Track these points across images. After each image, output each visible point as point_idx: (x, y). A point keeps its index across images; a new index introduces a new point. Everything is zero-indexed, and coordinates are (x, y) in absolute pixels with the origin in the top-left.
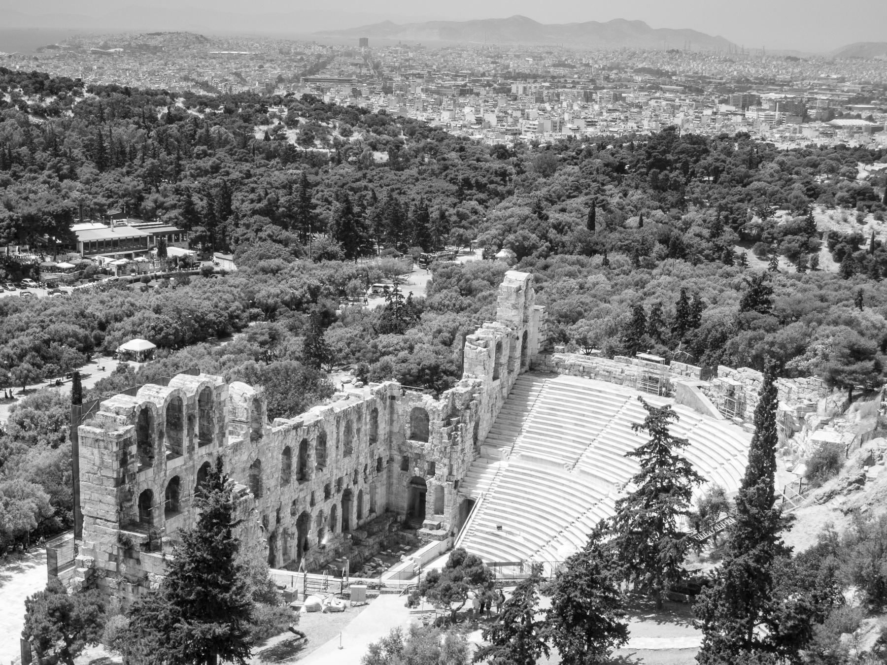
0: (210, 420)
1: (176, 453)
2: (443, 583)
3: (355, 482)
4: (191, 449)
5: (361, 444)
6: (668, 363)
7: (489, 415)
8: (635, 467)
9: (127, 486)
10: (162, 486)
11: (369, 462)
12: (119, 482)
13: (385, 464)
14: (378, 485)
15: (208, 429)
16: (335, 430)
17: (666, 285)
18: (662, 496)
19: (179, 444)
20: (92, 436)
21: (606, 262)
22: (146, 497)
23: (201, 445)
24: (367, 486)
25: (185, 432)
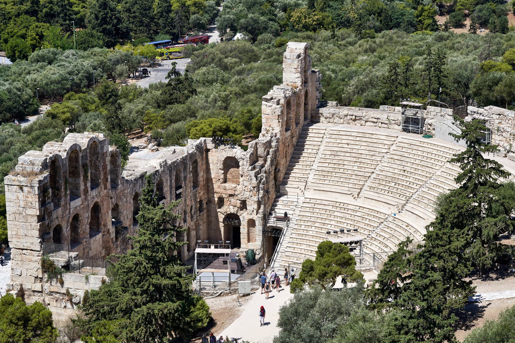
0: (96, 168)
1: (74, 196)
2: (319, 269)
3: (185, 221)
4: (86, 191)
5: (187, 190)
6: (425, 109)
7: (284, 160)
8: (457, 169)
9: (47, 222)
10: (68, 221)
11: (193, 203)
12: (41, 218)
13: (205, 206)
14: (201, 223)
15: (96, 176)
16: (168, 178)
17: (409, 47)
18: (481, 189)
19: (77, 188)
20: (17, 183)
21: (334, 36)
22: (58, 230)
23: (92, 189)
24: (192, 223)
25: (82, 178)
